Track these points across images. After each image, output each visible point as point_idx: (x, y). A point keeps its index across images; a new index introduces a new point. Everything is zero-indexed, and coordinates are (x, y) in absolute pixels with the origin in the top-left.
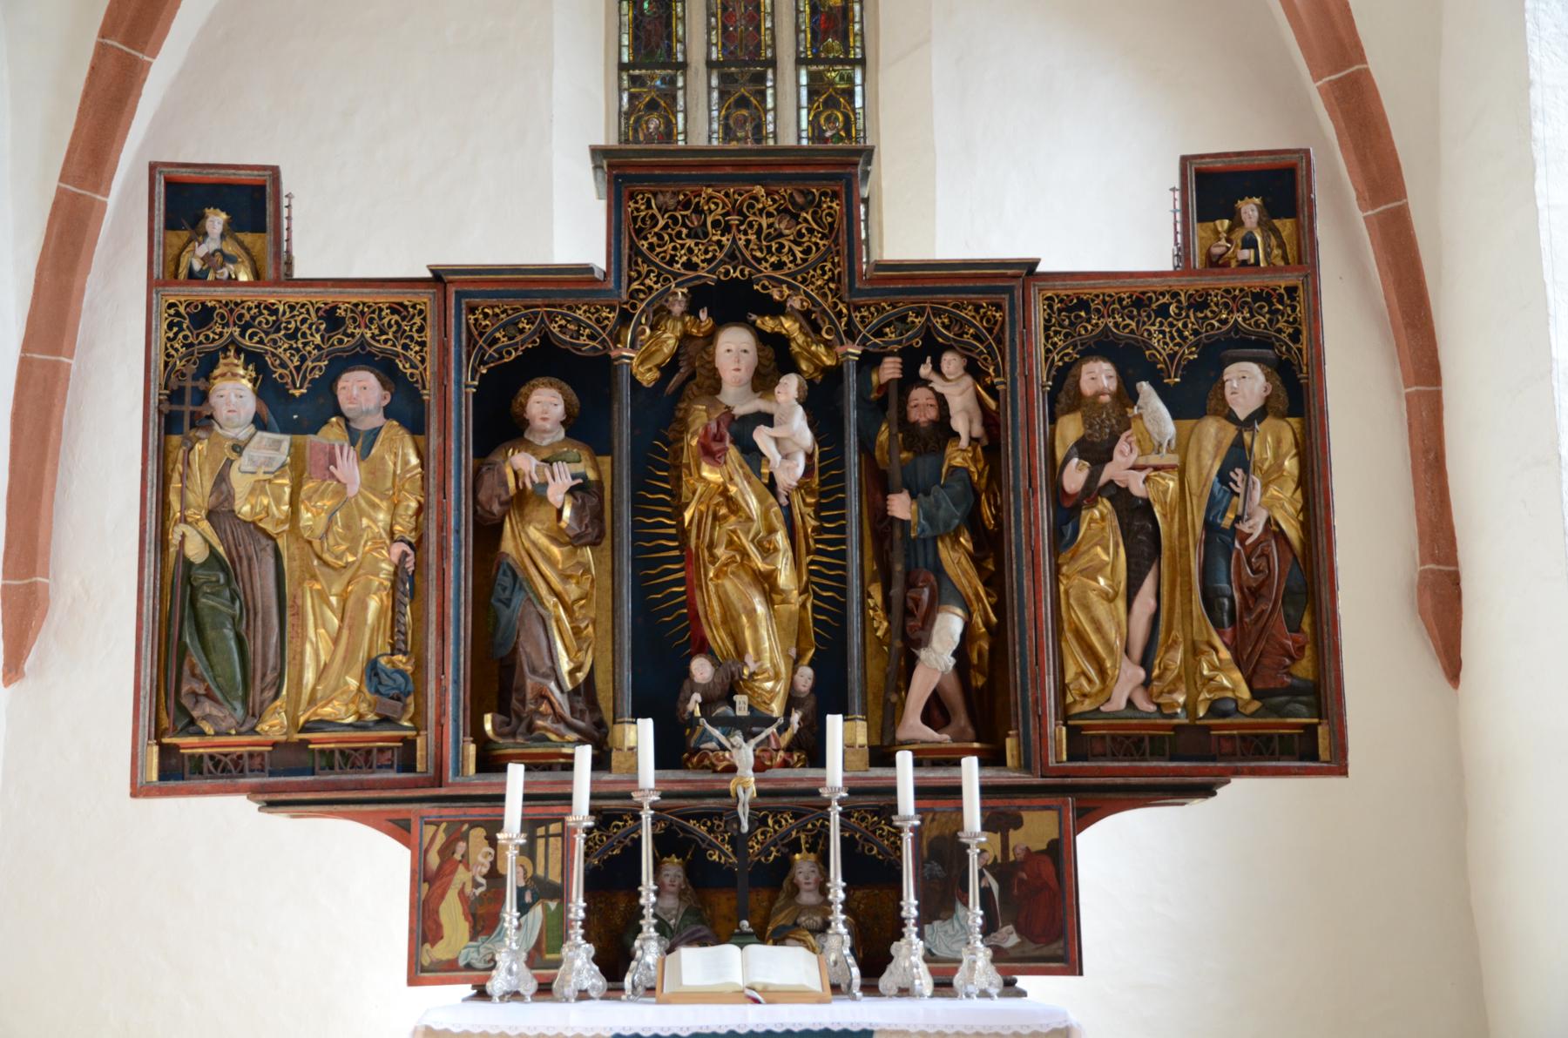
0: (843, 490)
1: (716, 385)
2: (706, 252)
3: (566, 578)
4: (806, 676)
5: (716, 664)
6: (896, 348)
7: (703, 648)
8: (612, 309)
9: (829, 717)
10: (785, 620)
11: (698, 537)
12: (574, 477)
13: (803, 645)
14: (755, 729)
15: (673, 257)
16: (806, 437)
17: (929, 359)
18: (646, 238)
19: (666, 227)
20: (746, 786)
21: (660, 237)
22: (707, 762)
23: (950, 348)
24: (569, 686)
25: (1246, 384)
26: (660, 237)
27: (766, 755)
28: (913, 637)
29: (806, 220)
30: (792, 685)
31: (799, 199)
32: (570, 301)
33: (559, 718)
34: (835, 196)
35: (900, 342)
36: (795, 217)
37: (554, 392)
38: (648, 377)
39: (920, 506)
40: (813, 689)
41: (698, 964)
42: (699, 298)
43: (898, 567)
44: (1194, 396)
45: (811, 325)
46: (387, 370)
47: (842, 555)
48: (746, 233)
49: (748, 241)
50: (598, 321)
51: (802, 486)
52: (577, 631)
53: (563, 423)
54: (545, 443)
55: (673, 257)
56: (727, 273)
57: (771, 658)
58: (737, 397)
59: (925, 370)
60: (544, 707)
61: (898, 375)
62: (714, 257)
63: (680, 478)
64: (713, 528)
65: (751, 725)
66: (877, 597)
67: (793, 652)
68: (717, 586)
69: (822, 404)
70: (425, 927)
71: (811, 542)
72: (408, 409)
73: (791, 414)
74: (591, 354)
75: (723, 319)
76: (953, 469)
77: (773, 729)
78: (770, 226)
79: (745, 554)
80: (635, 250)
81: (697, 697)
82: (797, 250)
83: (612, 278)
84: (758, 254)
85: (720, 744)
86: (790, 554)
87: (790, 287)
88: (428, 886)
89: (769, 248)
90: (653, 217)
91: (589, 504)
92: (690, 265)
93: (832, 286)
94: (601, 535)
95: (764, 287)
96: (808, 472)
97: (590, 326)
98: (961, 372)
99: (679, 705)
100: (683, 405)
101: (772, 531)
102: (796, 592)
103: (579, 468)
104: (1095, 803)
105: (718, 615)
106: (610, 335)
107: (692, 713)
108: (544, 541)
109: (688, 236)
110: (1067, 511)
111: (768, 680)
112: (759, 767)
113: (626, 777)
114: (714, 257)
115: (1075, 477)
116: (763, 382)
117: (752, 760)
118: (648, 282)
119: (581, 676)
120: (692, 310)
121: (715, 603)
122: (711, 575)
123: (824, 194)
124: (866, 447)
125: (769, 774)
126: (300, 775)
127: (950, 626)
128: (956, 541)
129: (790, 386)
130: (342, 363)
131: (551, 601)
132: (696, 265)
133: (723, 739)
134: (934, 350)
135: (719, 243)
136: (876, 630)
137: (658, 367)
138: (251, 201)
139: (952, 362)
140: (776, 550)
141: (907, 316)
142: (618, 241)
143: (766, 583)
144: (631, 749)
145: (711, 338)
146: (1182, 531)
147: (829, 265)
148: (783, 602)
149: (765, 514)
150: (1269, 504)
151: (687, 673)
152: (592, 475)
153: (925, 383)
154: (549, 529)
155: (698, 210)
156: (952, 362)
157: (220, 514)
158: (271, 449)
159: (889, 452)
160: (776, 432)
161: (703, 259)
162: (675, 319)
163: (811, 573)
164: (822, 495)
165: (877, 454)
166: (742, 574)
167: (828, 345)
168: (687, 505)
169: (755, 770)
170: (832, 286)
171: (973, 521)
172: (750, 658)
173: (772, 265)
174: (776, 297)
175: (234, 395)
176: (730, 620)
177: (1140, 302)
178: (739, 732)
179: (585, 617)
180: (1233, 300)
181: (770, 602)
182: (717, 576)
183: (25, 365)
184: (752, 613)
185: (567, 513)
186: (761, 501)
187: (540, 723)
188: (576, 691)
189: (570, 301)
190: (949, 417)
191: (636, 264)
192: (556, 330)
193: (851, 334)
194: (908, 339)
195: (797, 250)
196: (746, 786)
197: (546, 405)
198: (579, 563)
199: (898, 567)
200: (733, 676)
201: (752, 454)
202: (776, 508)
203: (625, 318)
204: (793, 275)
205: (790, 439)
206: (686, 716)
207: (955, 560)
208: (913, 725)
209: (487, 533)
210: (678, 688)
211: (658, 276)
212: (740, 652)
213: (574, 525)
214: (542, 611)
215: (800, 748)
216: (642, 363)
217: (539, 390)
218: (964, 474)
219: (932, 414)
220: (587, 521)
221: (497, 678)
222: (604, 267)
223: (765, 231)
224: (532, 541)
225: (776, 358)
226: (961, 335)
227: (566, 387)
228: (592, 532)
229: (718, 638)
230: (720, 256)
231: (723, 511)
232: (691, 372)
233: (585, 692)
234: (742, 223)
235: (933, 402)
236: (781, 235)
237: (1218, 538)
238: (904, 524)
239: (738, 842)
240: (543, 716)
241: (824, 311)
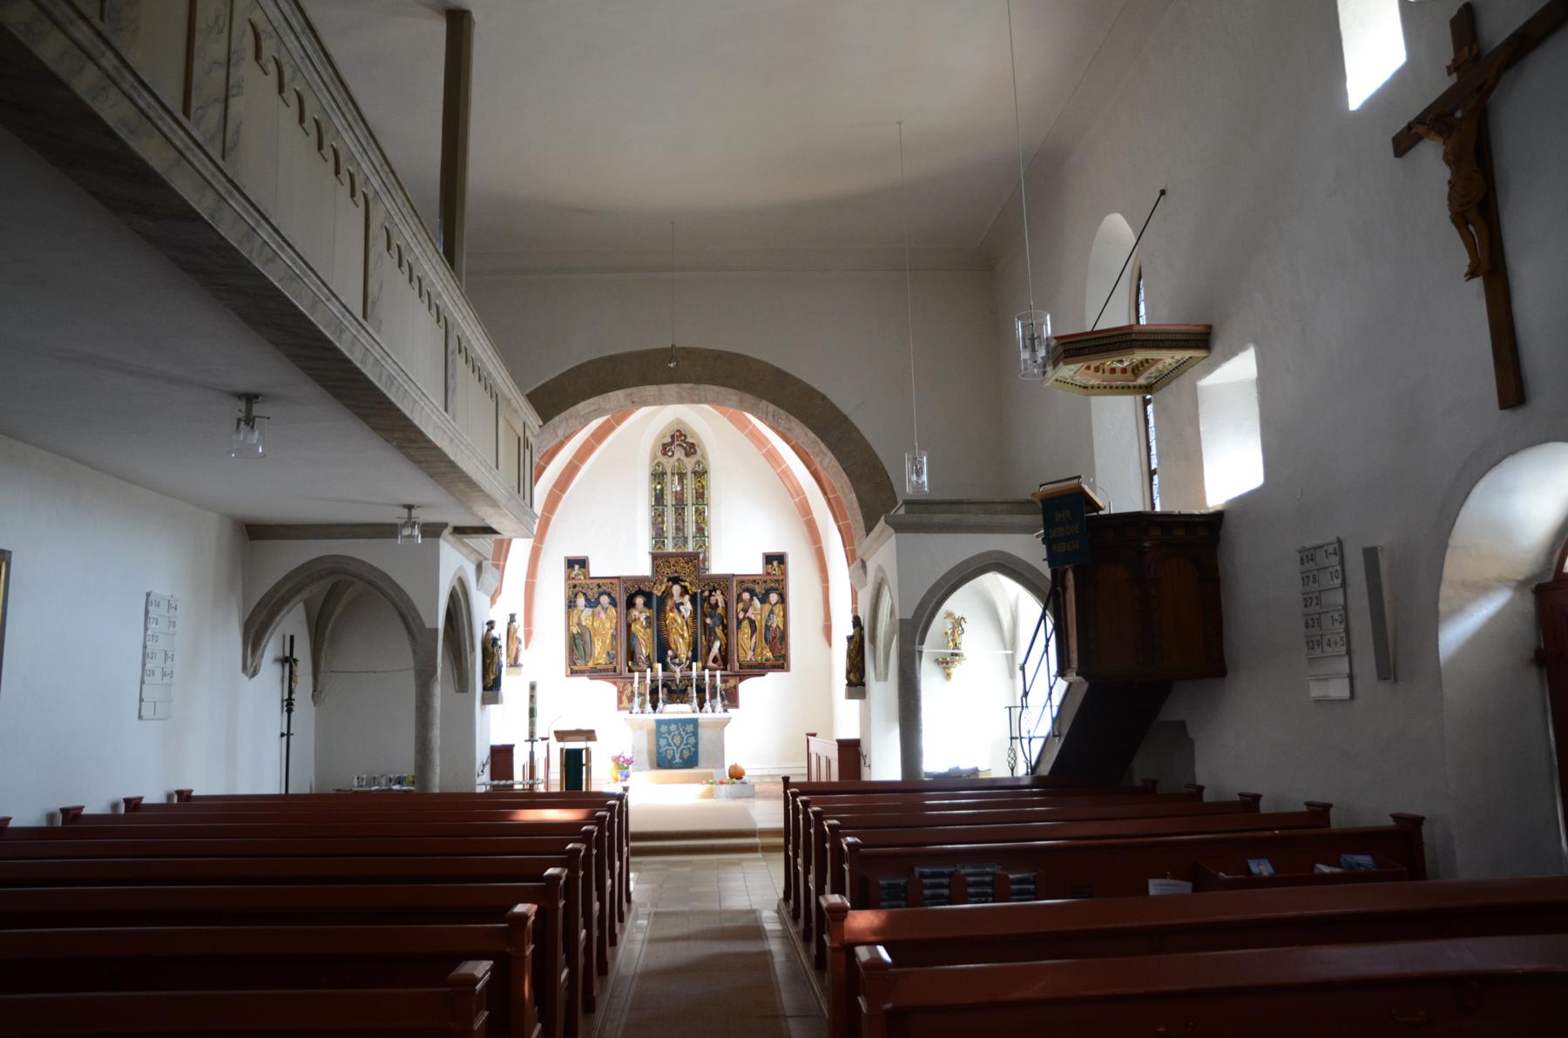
20: (678, 675)
25: (774, 597)
44: (764, 600)
46: (609, 595)
57: (684, 652)
58: (677, 598)
69: (693, 600)
70: (620, 701)
72: (613, 603)
88: (620, 693)
104: (742, 678)
110: (740, 622)
115: (741, 615)
116: (682, 595)
126: (596, 673)
127: (717, 644)
130: (601, 594)
138: (583, 563)
146: (760, 625)
150: (777, 621)
157: (579, 624)
158: (588, 611)
161: (670, 572)
175: (581, 601)
196: (678, 675)
197: (639, 601)
205: (687, 608)
207: (719, 631)
208: (710, 664)
209: (629, 626)
221: (631, 655)
224: (636, 628)
225: (685, 591)
232: (667, 594)
237: (767, 627)
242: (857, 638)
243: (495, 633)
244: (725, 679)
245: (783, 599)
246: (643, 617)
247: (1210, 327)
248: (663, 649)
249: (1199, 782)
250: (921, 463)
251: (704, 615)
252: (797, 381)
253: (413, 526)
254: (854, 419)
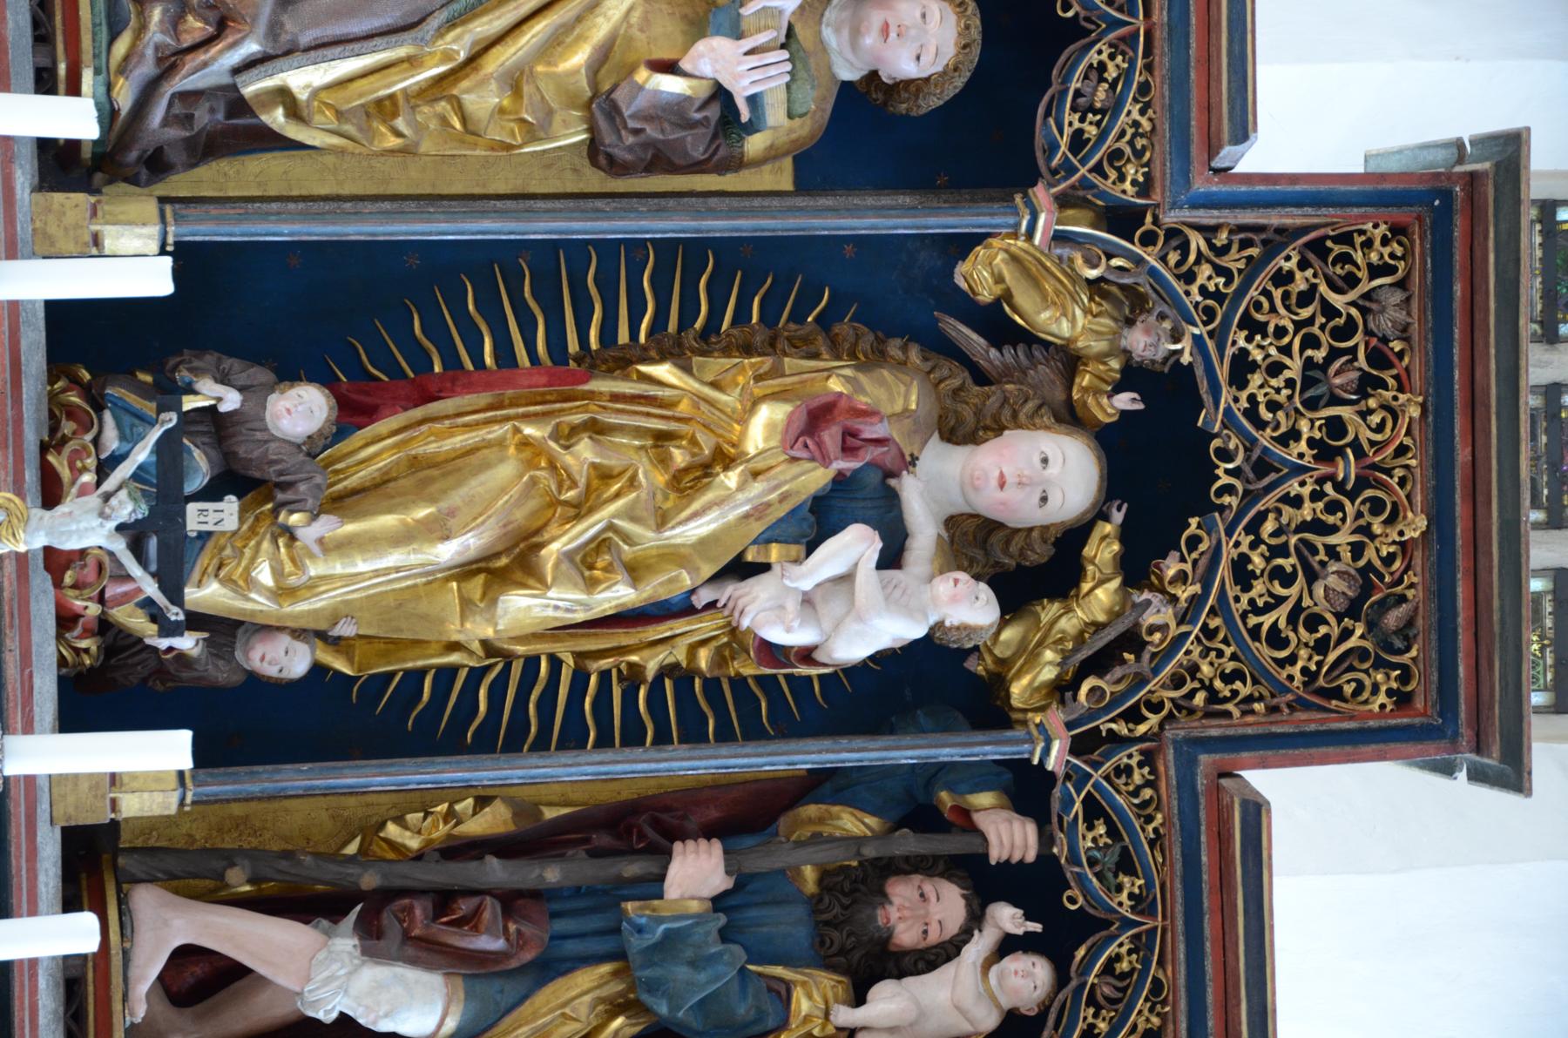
0: (725, 735)
1: (958, 432)
2: (1273, 406)
3: (514, 82)
4: (287, 660)
5: (313, 447)
6: (1060, 850)
7: (353, 412)
8: (1144, 188)
9: (184, 737)
10: (423, 607)
11: (616, 397)
12: (753, 100)
13: (360, 650)
14: (153, 544)
15: (1261, 328)
16: (852, 647)
17: (1036, 927)
18: (1303, 265)
19: (1329, 311)
21: (1306, 298)
22: (68, 427)
23: (1061, 977)
24: (252, 87)
26: (1306, 298)
27: (90, 573)
28: (387, 918)
29: (1346, 634)
30: (266, 629)
31: (1393, 618)
32: (1160, 90)
33: (169, 63)
34: (1402, 699)
35: (1074, 859)
36: (1353, 610)
37: (949, 52)
38: (979, 275)
39: (699, 919)
40: (254, 679)
42: (1168, 390)
43: (552, 874)
45: (1114, 649)
47: (573, 739)
48: (1316, 496)
49: (1296, 502)
50: (1116, 155)
51: (736, 640)
52: (385, 108)
53: (873, 75)
54: (828, 34)
55: (1261, 328)
56: (1225, 455)
58: (937, 482)
59: (1007, 918)
60: (196, 27)
61: (996, 855)
62: (1261, 425)
63: (747, 350)
64: (638, 432)
65: (162, 540)
66: (479, 825)
67: (345, 629)
68: (500, 443)
69: (929, 682)
71: (605, 663)
73: (909, 612)
74: (1039, 141)
75: (1112, 442)
76: (782, 994)
77: (151, 589)
78: (1332, 552)
79: (579, 510)
80: (1277, 239)
81: (231, 400)
82: (1281, 615)
83: (1217, 187)
84: (1269, 526)
85: (116, 460)
86: (580, 617)
87: (1196, 602)
89: (1282, 551)
90: (1352, 281)
91: (688, 137)
92: (1242, 368)
93: (1200, 699)
94: (615, 167)
95: (1194, 542)
96: (771, 652)
97: (1102, 137)
98: (1006, 1004)
99: (210, 359)
100: (914, 355)
101: (635, 572)
102: (489, 632)
103: (775, 115)
105: (432, 448)
106: (1085, 184)
107: (191, 390)
108: (601, 28)
109: (1309, 364)
111: (278, 573)
112: (56, 561)
113: (23, 228)
114: (1261, 425)
116: (974, 542)
117: (72, 544)
118: (1206, 270)
119: (276, 118)
120: (1133, 376)
121: (459, 441)
122: (529, 430)
123: (1405, 678)
124: (819, 784)
125: (41, 581)
128: (616, 1007)
129: (968, 607)
131: (459, 44)
132: (1243, 385)
133: (125, 470)
134: (1059, 936)
135: (1294, 434)
136: (400, 820)
137: (1007, 296)
139: (1028, 979)
140: (591, 584)
141: (1132, 872)
142: (1299, 201)
143: (513, 562)
144: (96, 240)
145: (1070, 417)
147: (1245, 690)
148: (466, 604)
149: (675, 557)
151: (288, 375)
152: (755, 144)
153: (975, 919)
154: (629, 40)
155: (1367, 385)
156: (1028, 979)
159: (816, 839)
160: (867, 574)
162: (1116, 335)
163: (532, 662)
164: (712, 685)
165: (812, 810)
166: (533, 504)
167: (1062, 689)
168: (687, 369)
169: (48, 551)
170: (1200, 699)
172: (327, 526)
173: (1244, 559)
174: (1171, 567)
176: (423, 476)
178: (143, 511)
179: (419, 128)
181: (465, 571)
182: (525, 443)
184: (439, 530)
185: (671, 85)
186: (703, 544)
187: (156, 14)
188: (239, 106)
189: (1160, 90)
190: (900, 975)
191: (1245, 244)
192: (1093, 57)
193: (1082, 745)
194: (1080, 879)
195: (1281, 615)
198: (550, 113)
199: (552, 874)
200: (285, 486)
202: (687, 581)
203: (1122, 219)
204: (1221, 608)
205: (851, 608)
206: (183, 375)
208: (168, 924)
210: (254, 356)
211: (1218, 296)
212: (341, 503)
213: (641, 102)
214: (434, 22)
215: (109, 651)
216: (1014, 259)
217: (952, 18)
218: (771, 1023)
219: (907, 936)
220: (652, 132)
222: (1241, 168)
223: (1318, 541)
225: (1029, 571)
226: (1092, 1001)
227: (960, 82)
228: (622, 145)
229: (376, 449)
230: (1265, 438)
231: (679, 457)
232: (990, 369)
233: (238, 130)
234: (1339, 487)
235: (934, 937)
236: (1312, 577)
238: (653, 885)
240: (174, 24)
241: (1141, 681)
251: (743, 816)
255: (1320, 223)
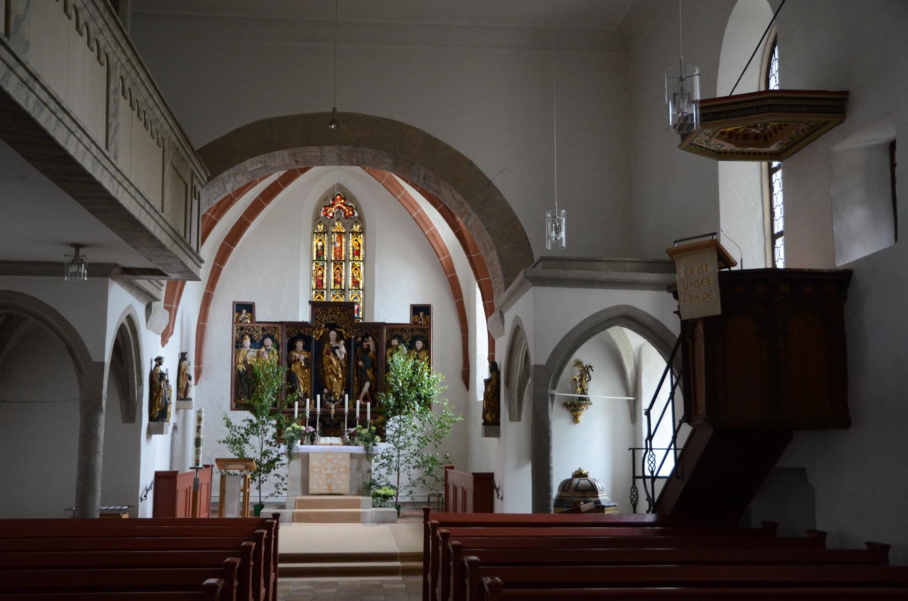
20: (333, 412)
41: (323, 440)
58: (333, 343)
65: (334, 402)
116: (338, 340)
120: (326, 327)
124: (355, 351)
127: (367, 385)
129: (342, 342)
130: (265, 337)
139: (370, 338)
143: (337, 376)
145: (329, 332)
156: (370, 338)
157: (245, 362)
171: (373, 366)
175: (247, 342)
176: (331, 382)
177: (402, 329)
180: (418, 330)
183: (198, 325)
196: (333, 412)
197: (300, 344)
201: (335, 354)
225: (340, 337)
229: (329, 386)
232: (325, 338)
239: (331, 420)
242: (494, 382)
243: (162, 368)
244: (374, 415)
245: (427, 347)
246: (303, 357)
247: (846, 93)
248: (319, 385)
249: (820, 527)
250: (560, 221)
252: (447, 148)
253: (80, 265)
254: (497, 183)
255: (314, 314)
